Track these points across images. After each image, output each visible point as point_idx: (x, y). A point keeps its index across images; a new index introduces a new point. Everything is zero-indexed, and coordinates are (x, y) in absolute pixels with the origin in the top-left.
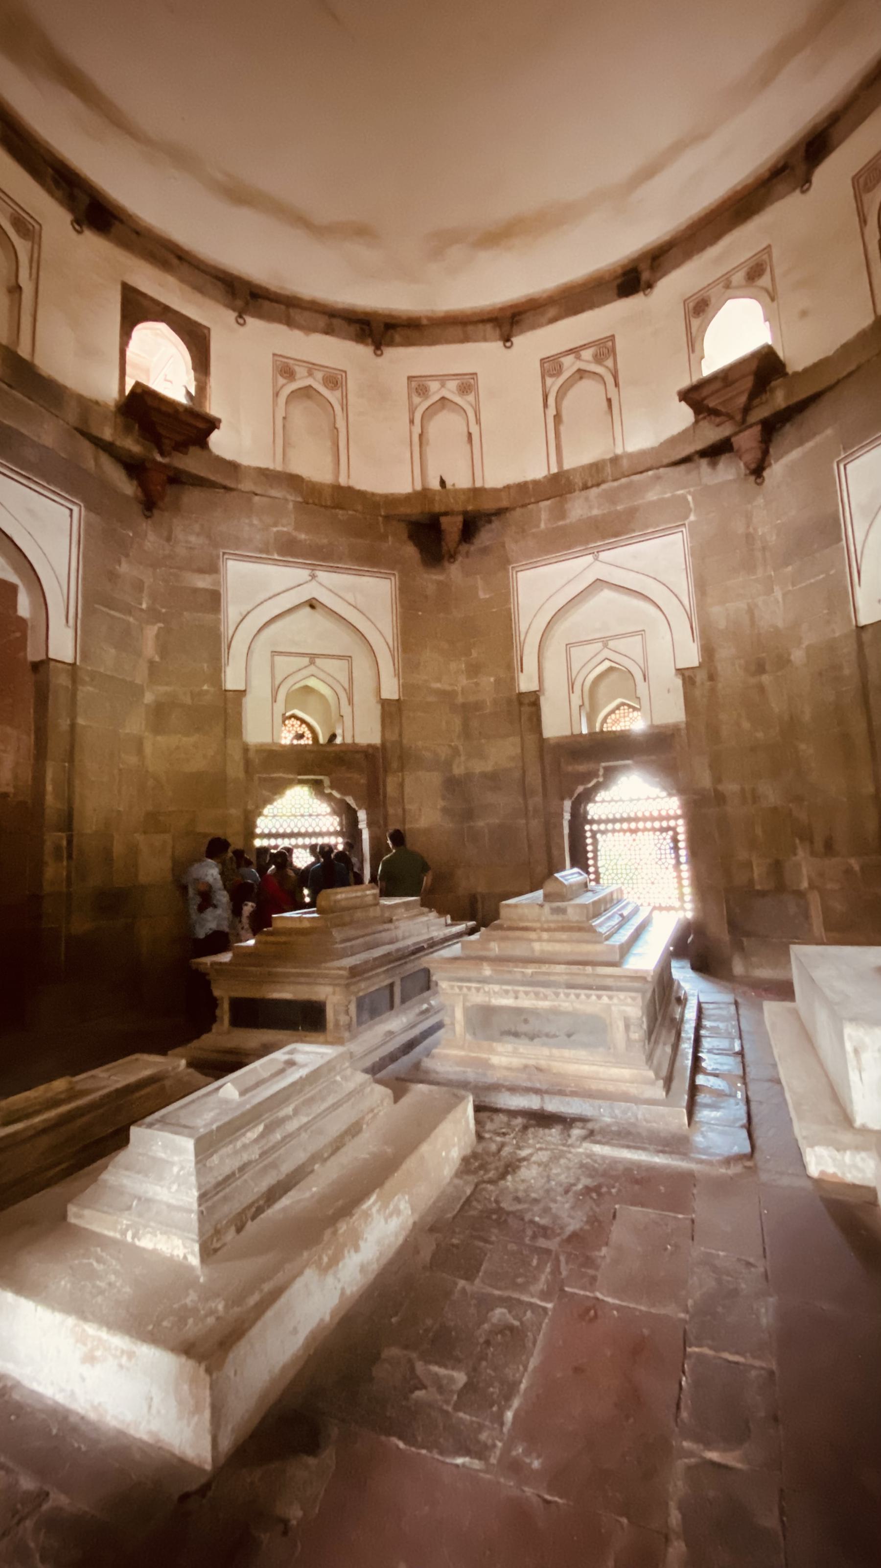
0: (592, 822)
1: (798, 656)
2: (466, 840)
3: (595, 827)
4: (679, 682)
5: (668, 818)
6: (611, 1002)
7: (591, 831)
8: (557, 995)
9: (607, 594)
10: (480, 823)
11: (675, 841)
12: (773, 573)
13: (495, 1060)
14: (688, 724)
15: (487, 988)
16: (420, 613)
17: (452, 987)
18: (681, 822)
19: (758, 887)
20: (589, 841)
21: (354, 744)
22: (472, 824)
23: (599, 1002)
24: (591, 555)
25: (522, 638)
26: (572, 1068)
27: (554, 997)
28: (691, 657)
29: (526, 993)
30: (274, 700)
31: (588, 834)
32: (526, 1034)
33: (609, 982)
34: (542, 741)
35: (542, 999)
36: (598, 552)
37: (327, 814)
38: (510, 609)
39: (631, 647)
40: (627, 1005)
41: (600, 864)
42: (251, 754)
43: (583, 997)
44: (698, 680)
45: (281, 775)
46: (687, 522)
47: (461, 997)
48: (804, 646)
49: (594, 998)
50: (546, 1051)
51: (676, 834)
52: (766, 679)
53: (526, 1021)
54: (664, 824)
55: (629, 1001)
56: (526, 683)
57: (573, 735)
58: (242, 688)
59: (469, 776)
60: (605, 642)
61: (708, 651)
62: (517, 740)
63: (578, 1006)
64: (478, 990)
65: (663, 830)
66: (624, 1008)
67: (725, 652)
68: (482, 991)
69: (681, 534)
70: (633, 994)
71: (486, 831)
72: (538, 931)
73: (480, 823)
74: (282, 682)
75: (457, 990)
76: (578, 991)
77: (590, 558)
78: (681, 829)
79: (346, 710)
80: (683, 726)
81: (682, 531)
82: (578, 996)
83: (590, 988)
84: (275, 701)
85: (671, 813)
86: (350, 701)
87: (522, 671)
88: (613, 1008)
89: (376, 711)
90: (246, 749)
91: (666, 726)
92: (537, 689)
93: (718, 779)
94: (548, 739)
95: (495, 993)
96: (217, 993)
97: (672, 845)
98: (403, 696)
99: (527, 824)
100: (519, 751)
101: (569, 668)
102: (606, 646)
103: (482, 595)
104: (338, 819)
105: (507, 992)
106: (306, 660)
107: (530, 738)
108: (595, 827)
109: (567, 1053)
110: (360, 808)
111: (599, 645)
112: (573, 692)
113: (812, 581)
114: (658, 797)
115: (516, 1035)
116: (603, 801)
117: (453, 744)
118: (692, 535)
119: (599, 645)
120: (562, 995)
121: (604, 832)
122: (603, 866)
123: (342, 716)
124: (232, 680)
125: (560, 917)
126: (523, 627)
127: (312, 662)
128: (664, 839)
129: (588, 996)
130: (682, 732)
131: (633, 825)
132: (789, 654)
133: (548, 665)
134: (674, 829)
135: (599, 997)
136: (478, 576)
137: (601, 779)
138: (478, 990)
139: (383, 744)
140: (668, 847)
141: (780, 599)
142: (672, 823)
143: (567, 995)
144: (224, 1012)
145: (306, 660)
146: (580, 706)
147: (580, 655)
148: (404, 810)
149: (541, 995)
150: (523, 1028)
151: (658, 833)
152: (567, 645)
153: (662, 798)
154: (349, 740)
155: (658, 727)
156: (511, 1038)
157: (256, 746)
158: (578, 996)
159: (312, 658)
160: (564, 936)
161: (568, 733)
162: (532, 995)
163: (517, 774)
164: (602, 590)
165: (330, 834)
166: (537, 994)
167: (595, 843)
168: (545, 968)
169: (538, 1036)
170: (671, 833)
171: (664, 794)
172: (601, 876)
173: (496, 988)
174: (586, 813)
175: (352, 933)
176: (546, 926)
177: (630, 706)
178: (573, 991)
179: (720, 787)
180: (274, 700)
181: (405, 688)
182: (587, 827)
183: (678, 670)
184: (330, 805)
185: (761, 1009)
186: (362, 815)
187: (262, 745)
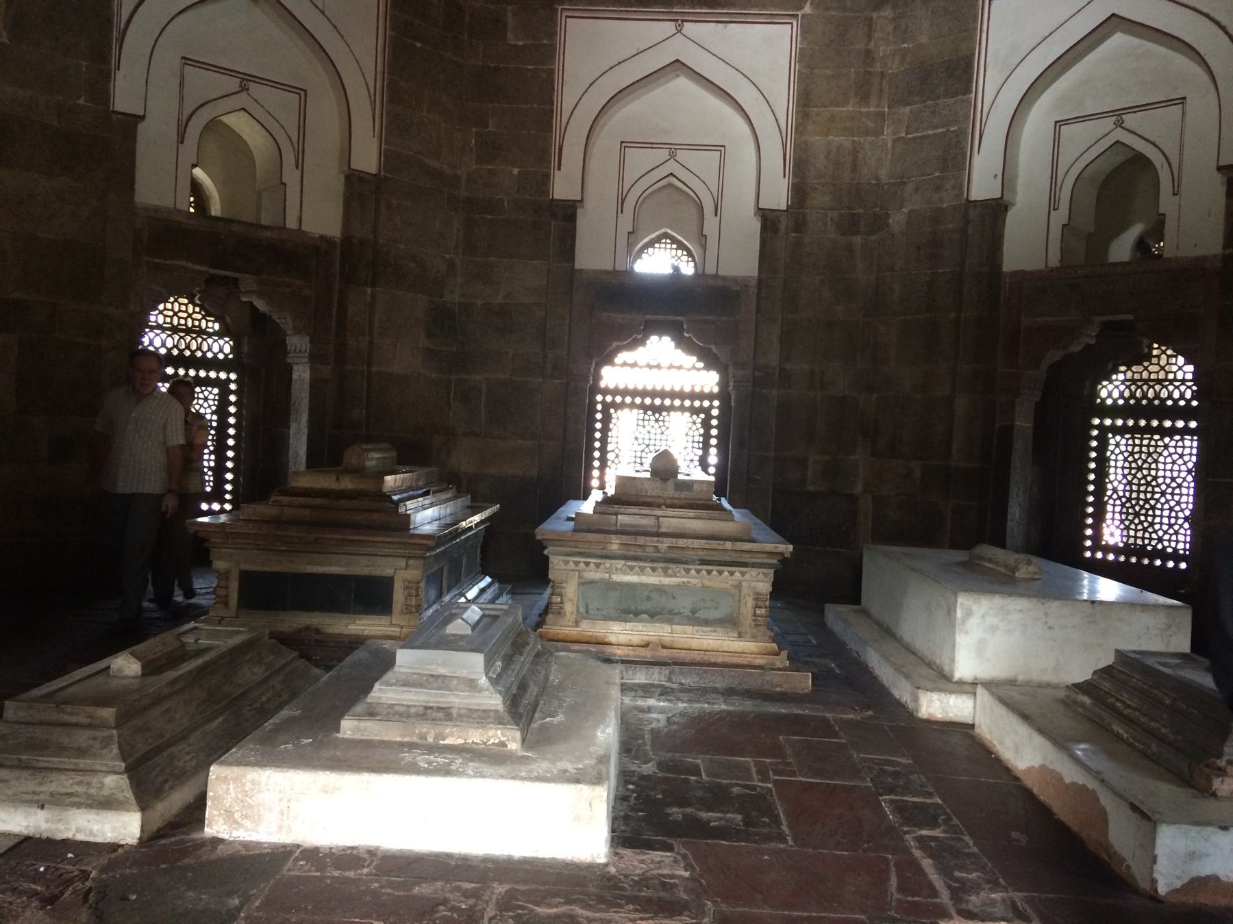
0: (605, 392)
1: (897, 220)
2: (452, 396)
3: (609, 399)
4: (757, 225)
5: (702, 396)
6: (743, 579)
7: (603, 403)
8: (688, 571)
9: (682, 83)
11: (706, 425)
12: (886, 109)
13: (612, 639)
14: (760, 281)
15: (608, 563)
16: (419, 45)
17: (567, 563)
18: (716, 403)
19: (811, 488)
20: (599, 416)
22: (466, 377)
23: (733, 578)
24: (674, 23)
25: (564, 120)
26: (695, 644)
27: (684, 573)
28: (778, 196)
29: (654, 570)
30: (181, 139)
31: (599, 407)
32: (646, 612)
33: (746, 558)
34: (572, 274)
35: (671, 576)
36: (683, 21)
37: (215, 333)
38: (553, 70)
39: (705, 163)
40: (758, 581)
41: (609, 448)
43: (715, 573)
44: (783, 226)
45: (183, 263)
46: (800, 13)
47: (577, 573)
48: (905, 210)
49: (726, 573)
50: (667, 628)
51: (709, 417)
52: (858, 240)
53: (648, 598)
54: (697, 404)
55: (761, 576)
56: (562, 187)
57: (615, 272)
58: (141, 113)
60: (674, 150)
61: (799, 191)
63: (707, 583)
64: (598, 565)
65: (694, 411)
66: (754, 584)
67: (820, 199)
68: (602, 566)
69: (790, 26)
70: (764, 570)
71: (484, 387)
72: (663, 507)
74: (194, 112)
75: (571, 565)
76: (710, 567)
77: (670, 27)
78: (715, 412)
79: (291, 176)
80: (754, 283)
81: (792, 23)
82: (709, 572)
83: (726, 564)
84: (182, 143)
85: (707, 390)
86: (299, 164)
87: (559, 169)
88: (744, 584)
89: (337, 185)
91: (735, 280)
92: (579, 198)
95: (617, 569)
97: (702, 431)
98: (384, 172)
101: (621, 179)
102: (672, 156)
103: (511, 39)
104: (231, 343)
106: (234, 84)
110: (298, 331)
111: (664, 154)
112: (622, 212)
113: (930, 132)
114: (694, 368)
115: (637, 614)
116: (625, 364)
118: (805, 32)
119: (664, 154)
120: (693, 572)
122: (613, 451)
123: (285, 184)
124: (124, 98)
126: (568, 104)
127: (244, 89)
128: (694, 423)
129: (720, 573)
130: (751, 290)
131: (658, 402)
132: (888, 216)
133: (593, 165)
135: (732, 573)
136: (510, 8)
138: (598, 565)
139: (347, 239)
140: (697, 433)
141: (890, 145)
142: (706, 404)
143: (698, 571)
145: (234, 84)
146: (629, 233)
147: (640, 160)
148: (371, 343)
149: (670, 572)
151: (687, 414)
152: (622, 142)
153: (698, 370)
154: (291, 223)
155: (724, 278)
157: (146, 210)
158: (709, 572)
159: (246, 80)
160: (691, 513)
161: (609, 267)
162: (660, 570)
164: (678, 76)
166: (665, 571)
167: (607, 419)
168: (681, 542)
169: (660, 613)
170: (702, 416)
171: (701, 365)
172: (609, 463)
173: (620, 563)
174: (598, 377)
176: (669, 501)
177: (674, 241)
178: (704, 567)
179: (788, 366)
180: (181, 139)
181: (388, 157)
182: (599, 398)
183: (759, 209)
185: (822, 611)
186: (298, 343)
187: (157, 210)
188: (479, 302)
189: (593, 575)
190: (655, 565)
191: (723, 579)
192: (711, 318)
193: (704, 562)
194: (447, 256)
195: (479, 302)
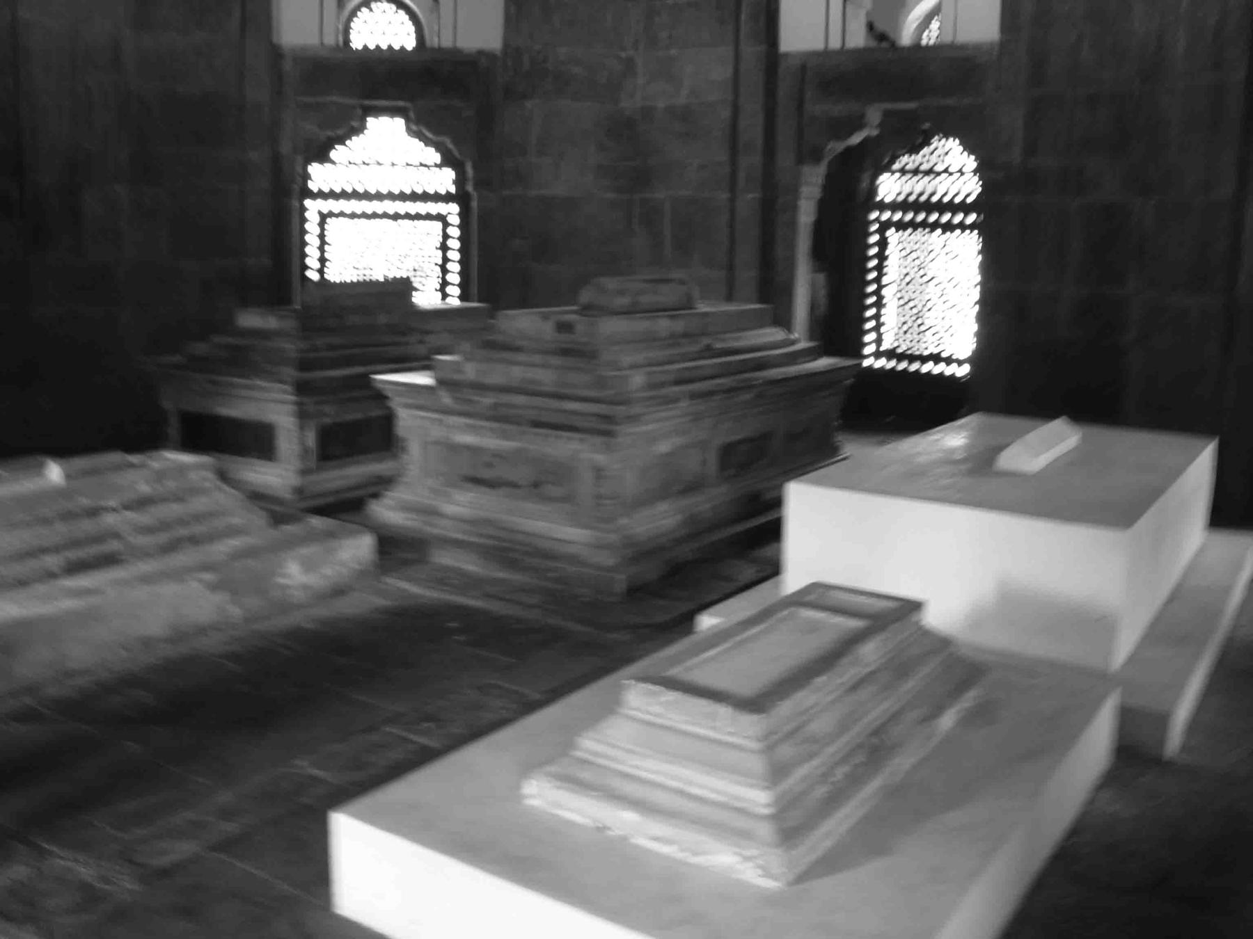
0: (882, 206)
3: (886, 216)
10: (660, 194)
13: (450, 509)
21: (455, 52)
33: (578, 422)
37: (436, 165)
41: (885, 280)
42: (287, 66)
45: (335, 98)
57: (826, 54)
59: (647, 112)
62: (726, 51)
73: (660, 194)
90: (276, 53)
91: (978, 47)
93: (1030, 150)
94: (787, 55)
96: (167, 405)
99: (732, 200)
100: (728, 72)
105: (468, 426)
107: (752, 51)
108: (886, 216)
109: (529, 506)
117: (623, 55)
121: (901, 226)
125: (564, 337)
134: (441, 218)
137: (875, 132)
144: (174, 429)
150: (487, 474)
155: (963, 47)
156: (470, 485)
161: (819, 45)
163: (726, 113)
165: (437, 198)
167: (883, 244)
174: (873, 190)
175: (336, 340)
184: (438, 150)
188: (661, 104)
189: (437, 432)
190: (495, 425)
191: (562, 447)
192: (950, 102)
193: (537, 424)
194: (623, 55)
195: (661, 104)
